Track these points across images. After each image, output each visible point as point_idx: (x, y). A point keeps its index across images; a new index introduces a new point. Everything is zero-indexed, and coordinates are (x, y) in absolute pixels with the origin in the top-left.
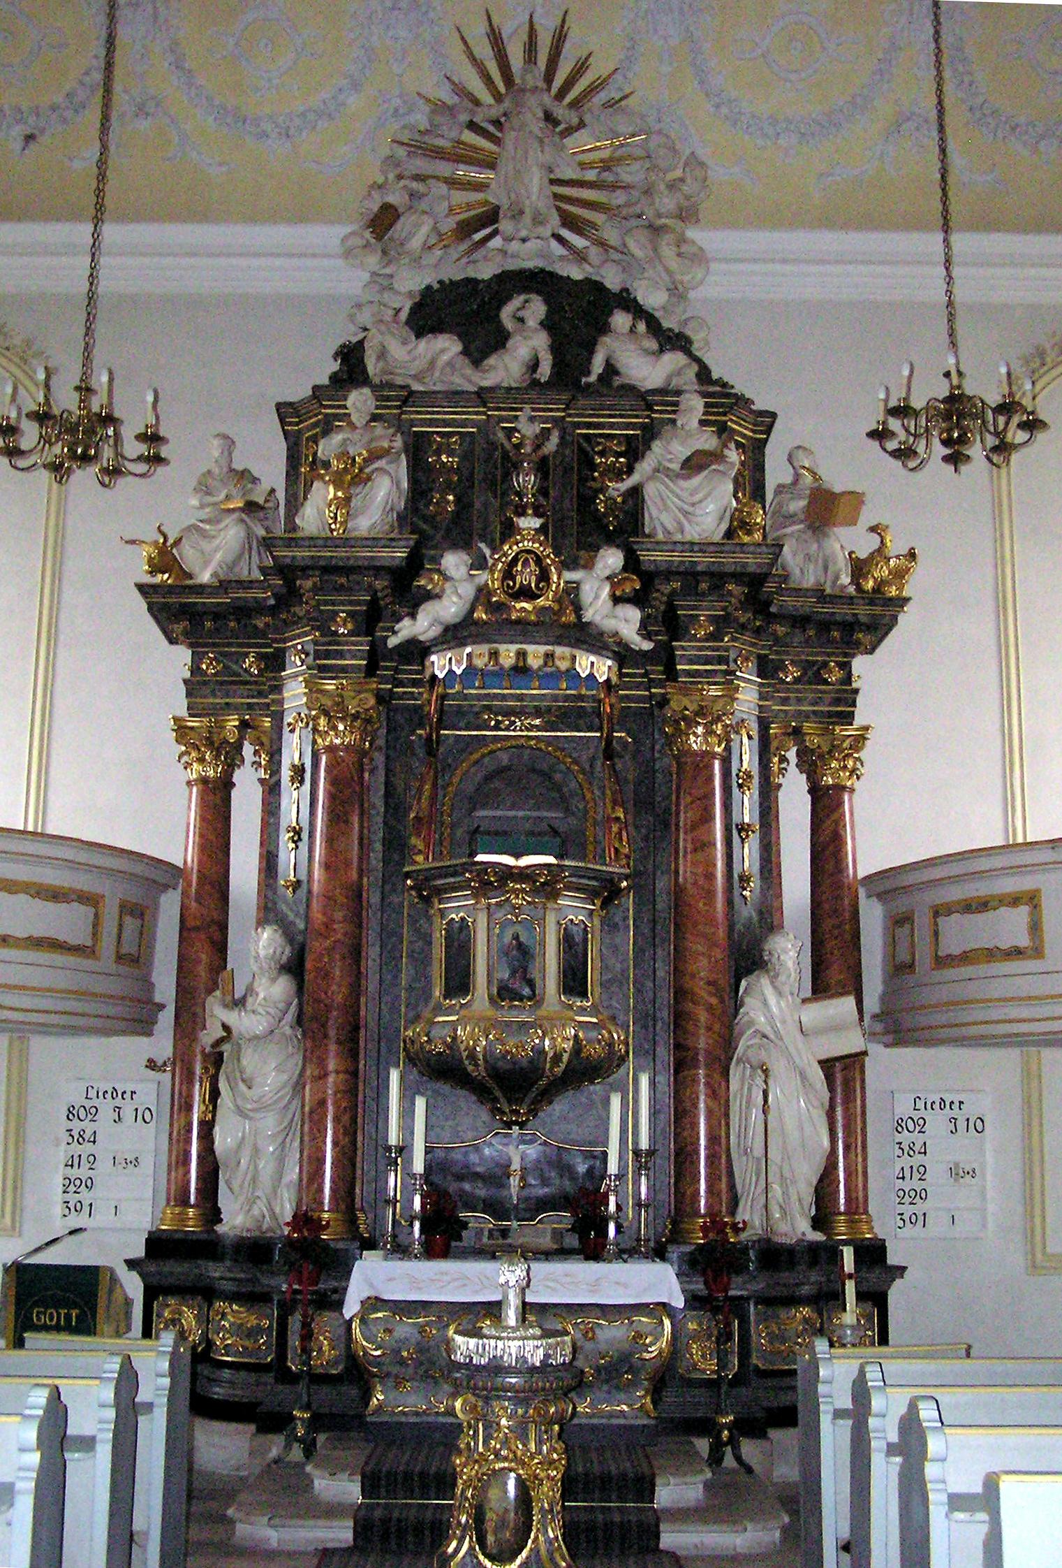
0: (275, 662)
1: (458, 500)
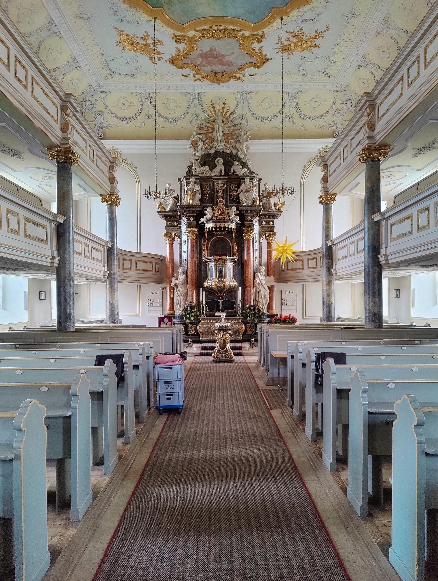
0: (180, 223)
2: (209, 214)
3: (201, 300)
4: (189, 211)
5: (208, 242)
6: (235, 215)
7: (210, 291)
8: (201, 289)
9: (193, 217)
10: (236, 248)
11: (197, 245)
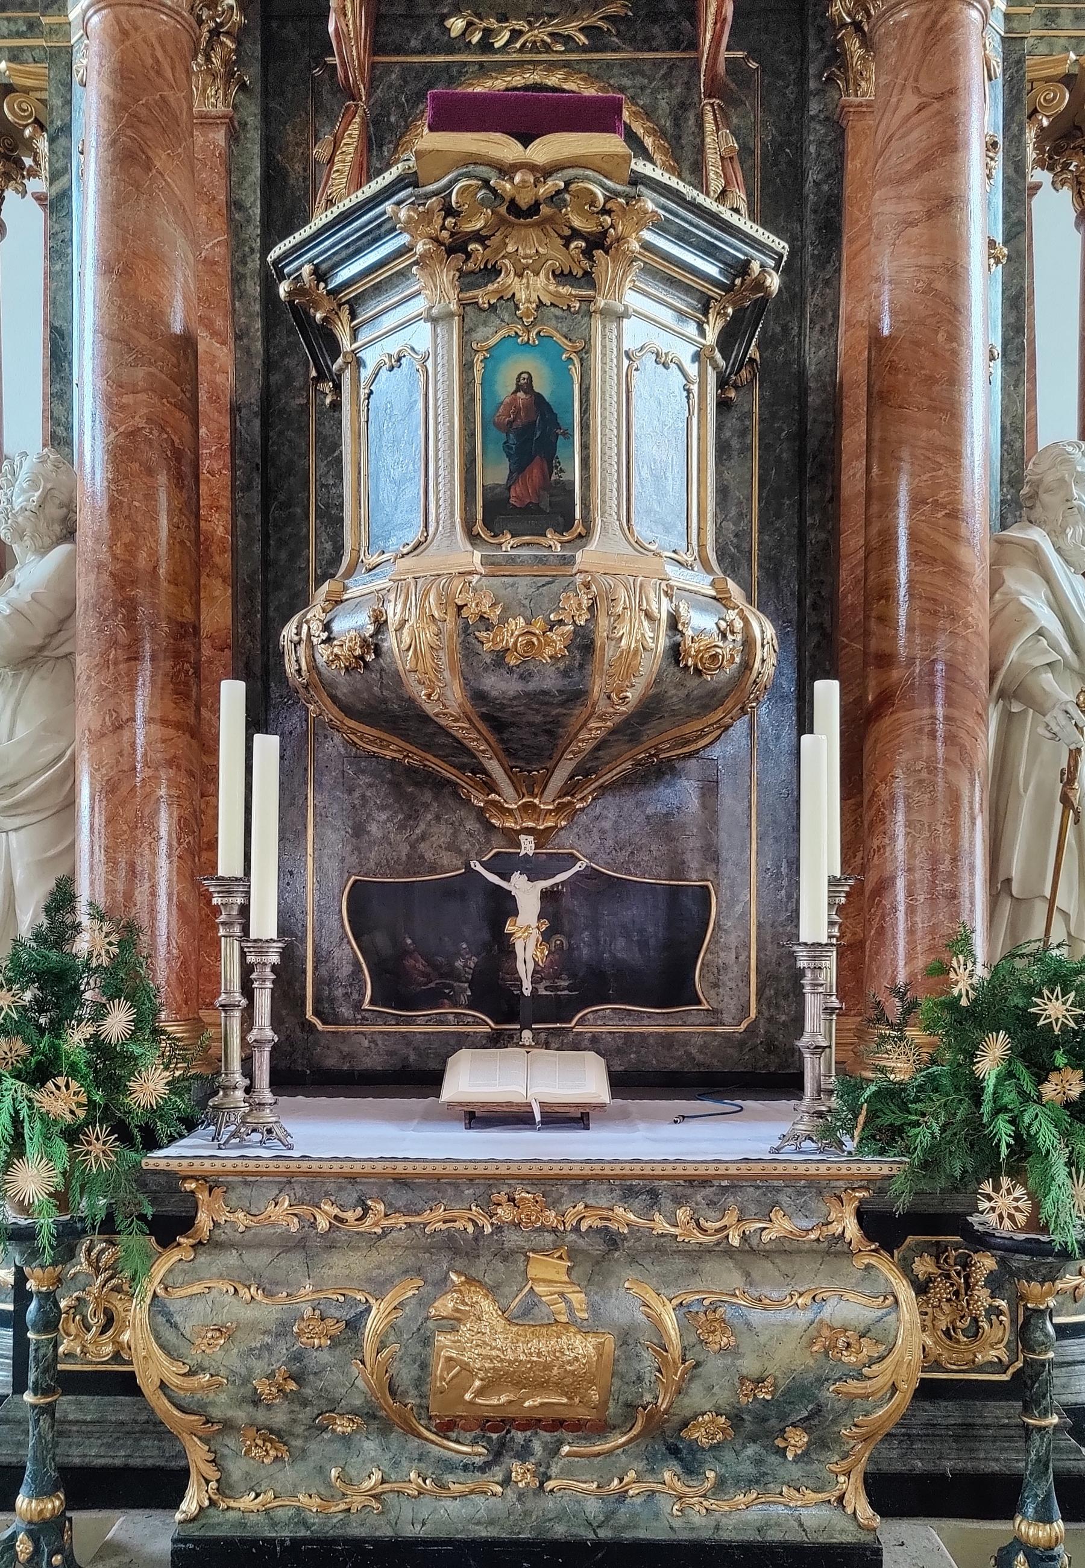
3: (228, 863)
8: (232, 695)
11: (232, 167)
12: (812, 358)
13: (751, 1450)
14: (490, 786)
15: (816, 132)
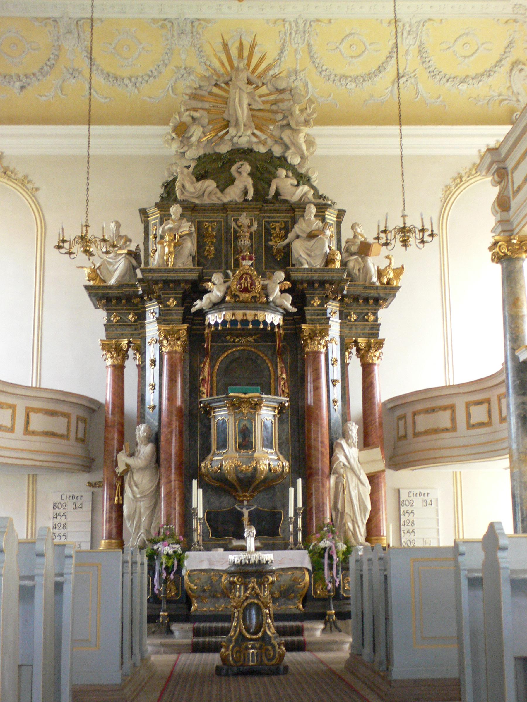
0: (141, 317)
1: (216, 249)
2: (216, 290)
4: (166, 282)
5: (213, 361)
6: (282, 292)
7: (219, 485)
9: (175, 299)
10: (284, 376)
12: (300, 404)
13: (283, 599)
14: (237, 491)
15: (299, 362)
